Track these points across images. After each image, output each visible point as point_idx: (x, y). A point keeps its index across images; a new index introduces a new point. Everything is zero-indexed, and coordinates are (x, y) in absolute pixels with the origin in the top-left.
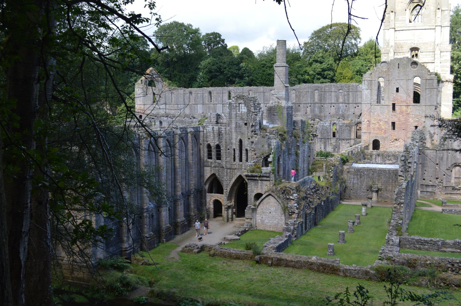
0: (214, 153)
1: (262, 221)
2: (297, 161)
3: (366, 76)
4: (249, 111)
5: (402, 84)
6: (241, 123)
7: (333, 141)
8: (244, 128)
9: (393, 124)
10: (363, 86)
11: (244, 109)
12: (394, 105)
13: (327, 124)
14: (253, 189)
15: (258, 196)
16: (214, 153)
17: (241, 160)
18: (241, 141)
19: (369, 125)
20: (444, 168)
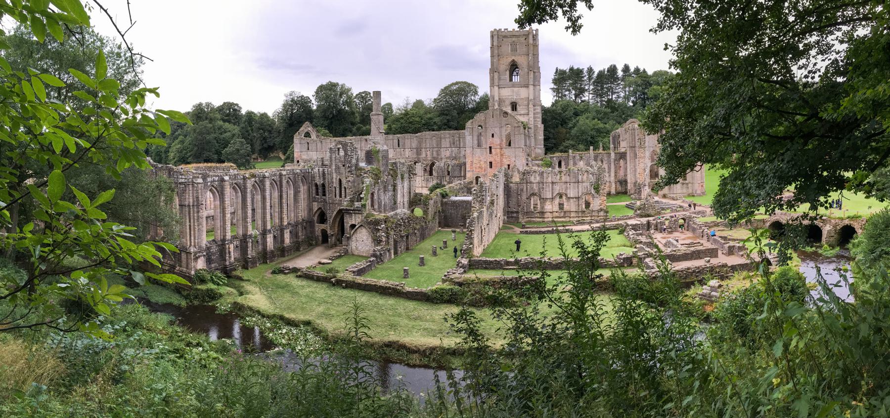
0: (320, 191)
1: (357, 248)
2: (395, 196)
3: (468, 124)
4: (346, 154)
5: (496, 131)
6: (340, 165)
7: (447, 178)
8: (342, 169)
9: (491, 163)
10: (466, 132)
11: (342, 153)
12: (490, 148)
13: (442, 165)
14: (349, 221)
15: (353, 226)
16: (320, 191)
17: (341, 196)
18: (340, 181)
19: (472, 165)
20: (524, 197)
